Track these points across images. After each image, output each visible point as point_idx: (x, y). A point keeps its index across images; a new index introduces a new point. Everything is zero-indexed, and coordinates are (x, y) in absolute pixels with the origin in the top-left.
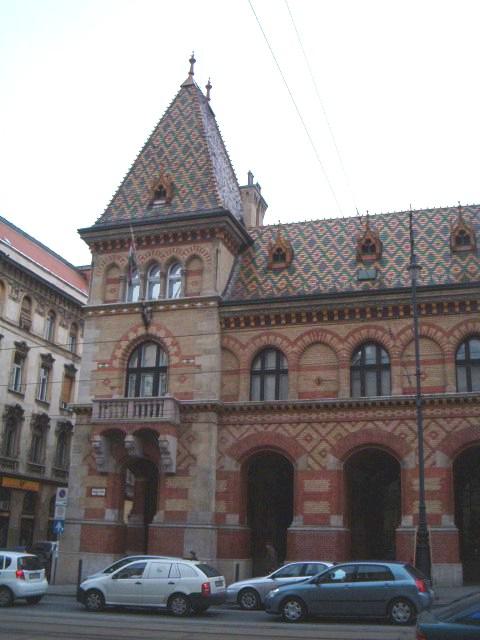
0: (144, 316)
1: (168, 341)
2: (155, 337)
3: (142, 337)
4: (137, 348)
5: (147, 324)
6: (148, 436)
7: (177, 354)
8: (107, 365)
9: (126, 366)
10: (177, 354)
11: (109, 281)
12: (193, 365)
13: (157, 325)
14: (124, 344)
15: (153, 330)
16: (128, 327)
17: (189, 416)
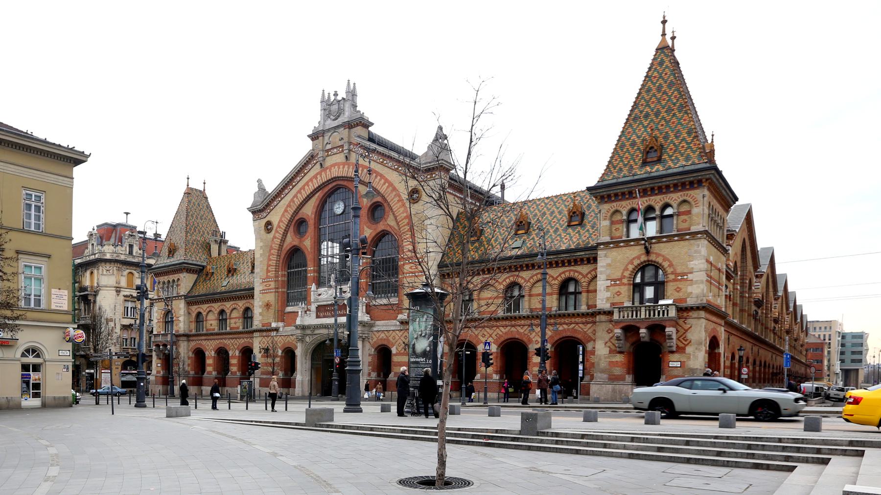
0: (646, 248)
1: (666, 264)
2: (655, 262)
3: (645, 262)
4: (642, 268)
5: (648, 252)
6: (657, 329)
7: (672, 273)
8: (618, 282)
9: (632, 282)
10: (672, 273)
12: (686, 280)
13: (656, 253)
14: (631, 267)
15: (653, 257)
16: (635, 253)
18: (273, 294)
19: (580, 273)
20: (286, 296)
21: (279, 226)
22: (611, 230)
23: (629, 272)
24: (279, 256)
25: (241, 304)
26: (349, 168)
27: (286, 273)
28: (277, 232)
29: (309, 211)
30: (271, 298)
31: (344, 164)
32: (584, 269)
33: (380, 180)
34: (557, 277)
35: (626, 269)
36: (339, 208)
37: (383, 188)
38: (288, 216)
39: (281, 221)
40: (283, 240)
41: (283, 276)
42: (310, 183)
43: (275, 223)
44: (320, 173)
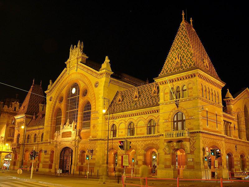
5: (178, 106)
11: (165, 94)
14: (172, 113)
17: (193, 135)
18: (50, 127)
19: (155, 117)
20: (55, 128)
21: (54, 99)
22: (164, 97)
23: (171, 116)
24: (53, 111)
25: (41, 131)
26: (77, 74)
27: (56, 118)
28: (53, 101)
29: (64, 92)
30: (49, 129)
31: (75, 73)
32: (156, 115)
33: (86, 79)
34: (146, 119)
35: (170, 115)
36: (74, 91)
37: (87, 82)
38: (57, 95)
39: (55, 97)
40: (55, 105)
41: (55, 119)
42: (65, 81)
43: (53, 98)
44: (68, 77)
